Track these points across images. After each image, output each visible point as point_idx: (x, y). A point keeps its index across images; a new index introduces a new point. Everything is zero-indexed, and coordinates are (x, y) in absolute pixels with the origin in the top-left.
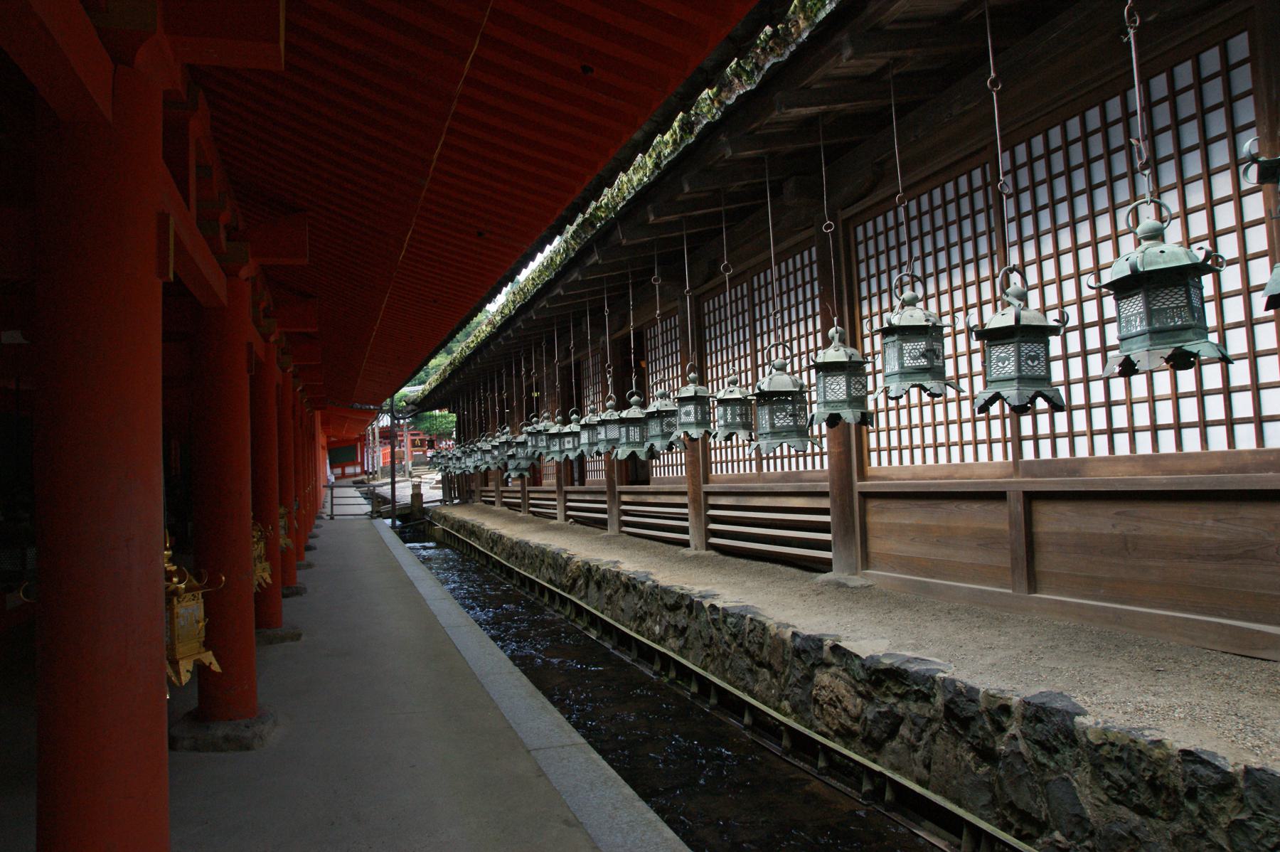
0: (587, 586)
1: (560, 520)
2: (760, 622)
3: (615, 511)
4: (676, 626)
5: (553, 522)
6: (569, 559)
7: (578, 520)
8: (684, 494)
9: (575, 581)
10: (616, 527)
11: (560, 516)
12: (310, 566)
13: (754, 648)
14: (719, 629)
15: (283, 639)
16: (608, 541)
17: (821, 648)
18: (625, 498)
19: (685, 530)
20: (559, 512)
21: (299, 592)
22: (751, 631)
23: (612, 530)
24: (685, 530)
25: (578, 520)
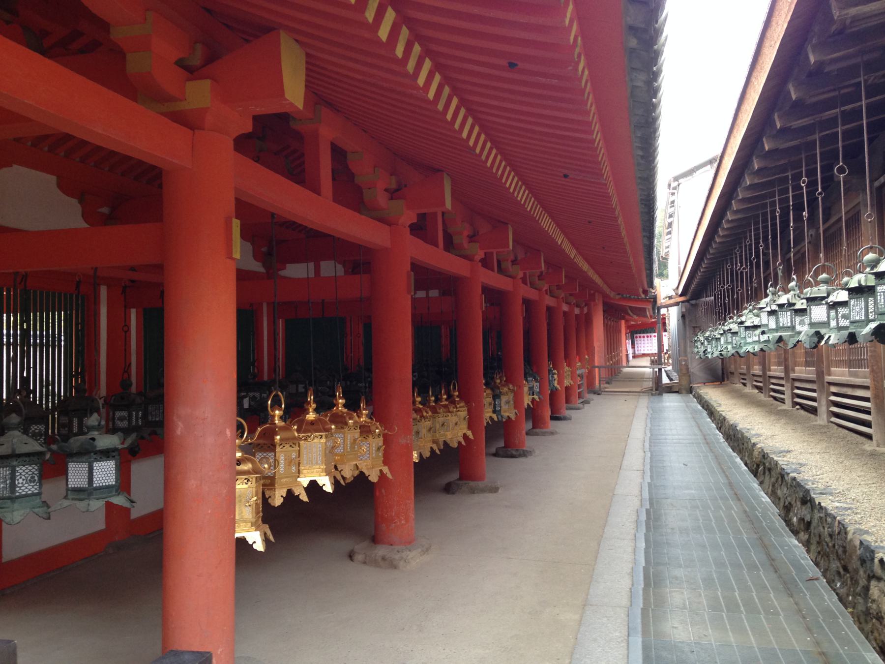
0: (764, 473)
1: (787, 406)
2: (843, 525)
3: (824, 402)
4: (803, 519)
5: (784, 407)
6: (754, 445)
7: (803, 407)
8: (866, 388)
9: (758, 466)
10: (825, 416)
11: (788, 402)
12: (552, 433)
13: (840, 551)
14: (824, 528)
15: (483, 491)
16: (814, 431)
17: (873, 559)
18: (833, 389)
19: (868, 424)
20: (787, 397)
21: (524, 454)
22: (839, 533)
23: (822, 419)
24: (868, 424)
25: (803, 407)
